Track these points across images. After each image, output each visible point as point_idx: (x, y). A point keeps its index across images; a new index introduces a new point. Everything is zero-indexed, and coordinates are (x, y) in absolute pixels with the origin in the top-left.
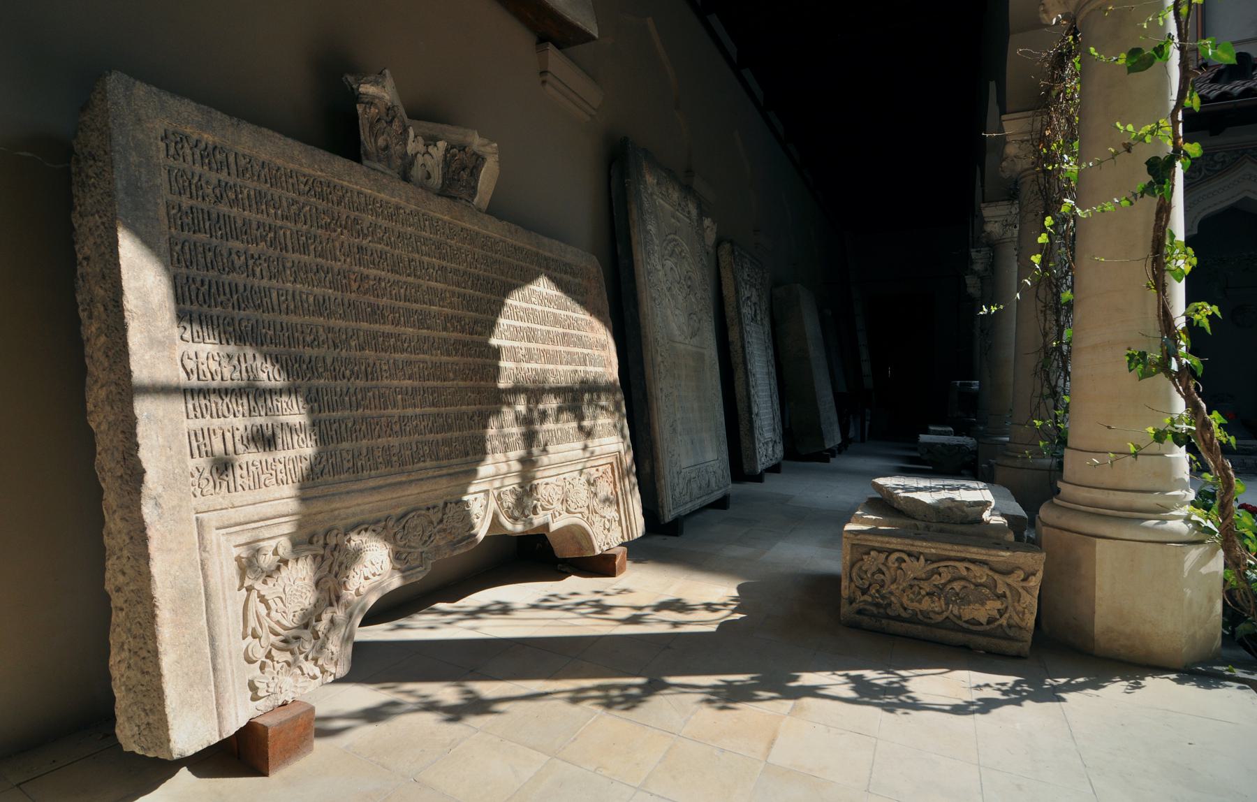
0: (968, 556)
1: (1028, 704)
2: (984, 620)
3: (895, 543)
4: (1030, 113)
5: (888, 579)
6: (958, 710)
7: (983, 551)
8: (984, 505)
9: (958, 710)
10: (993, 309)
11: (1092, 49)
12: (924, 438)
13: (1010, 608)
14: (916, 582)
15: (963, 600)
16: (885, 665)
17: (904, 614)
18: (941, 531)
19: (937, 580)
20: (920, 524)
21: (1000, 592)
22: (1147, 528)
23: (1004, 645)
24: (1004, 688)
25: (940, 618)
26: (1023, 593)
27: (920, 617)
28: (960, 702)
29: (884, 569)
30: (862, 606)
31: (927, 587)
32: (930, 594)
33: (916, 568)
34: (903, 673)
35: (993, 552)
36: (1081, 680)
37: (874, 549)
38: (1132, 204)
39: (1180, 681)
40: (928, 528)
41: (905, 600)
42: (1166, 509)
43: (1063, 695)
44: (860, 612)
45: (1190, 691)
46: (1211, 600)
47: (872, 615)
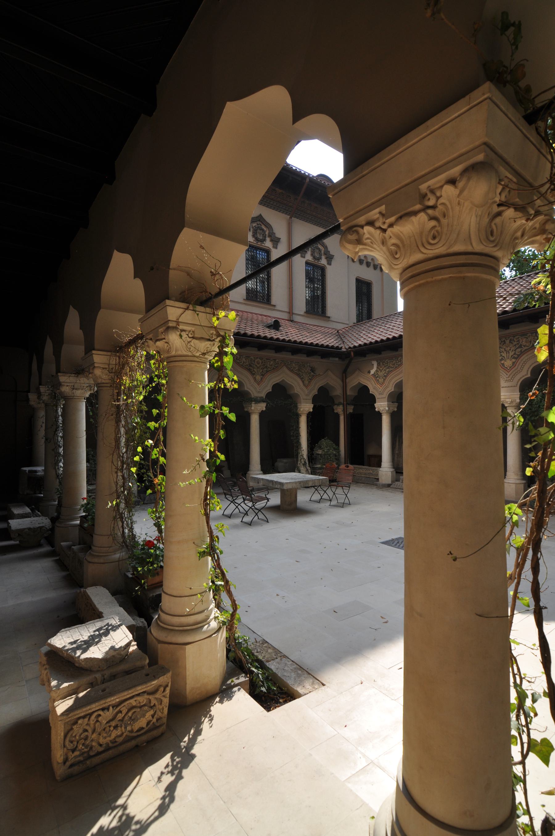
0: (137, 693)
1: (185, 772)
2: (144, 726)
3: (95, 706)
4: (109, 353)
5: (90, 731)
6: (163, 809)
7: (144, 686)
8: (128, 645)
9: (163, 809)
10: (114, 503)
11: (185, 399)
12: (15, 524)
13: (158, 711)
14: (108, 725)
15: (133, 720)
16: (108, 805)
17: (100, 749)
18: (113, 677)
19: (120, 716)
20: (98, 676)
21: (152, 705)
22: (205, 632)
23: (155, 733)
24: (170, 768)
25: (121, 739)
26: (163, 698)
27: (111, 745)
28: (159, 802)
29: (87, 728)
30: (73, 761)
31: (113, 724)
32: (116, 727)
33: (107, 715)
34: (120, 802)
35: (149, 684)
36: (192, 732)
37: (79, 718)
38: (201, 481)
39: (221, 702)
40: (103, 676)
41: (102, 741)
42: (208, 617)
43: (193, 752)
44: (71, 766)
45: (226, 703)
46: (223, 651)
47: (80, 762)
